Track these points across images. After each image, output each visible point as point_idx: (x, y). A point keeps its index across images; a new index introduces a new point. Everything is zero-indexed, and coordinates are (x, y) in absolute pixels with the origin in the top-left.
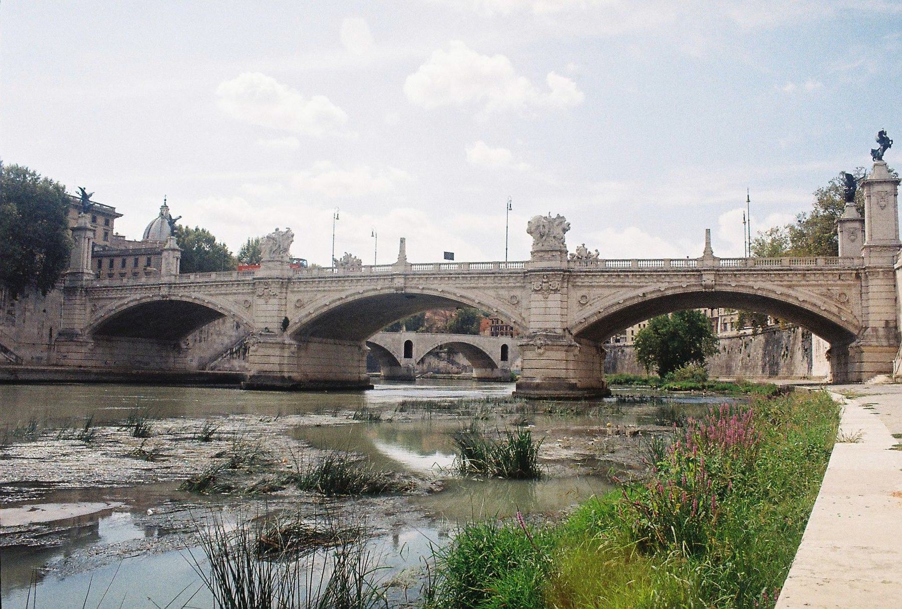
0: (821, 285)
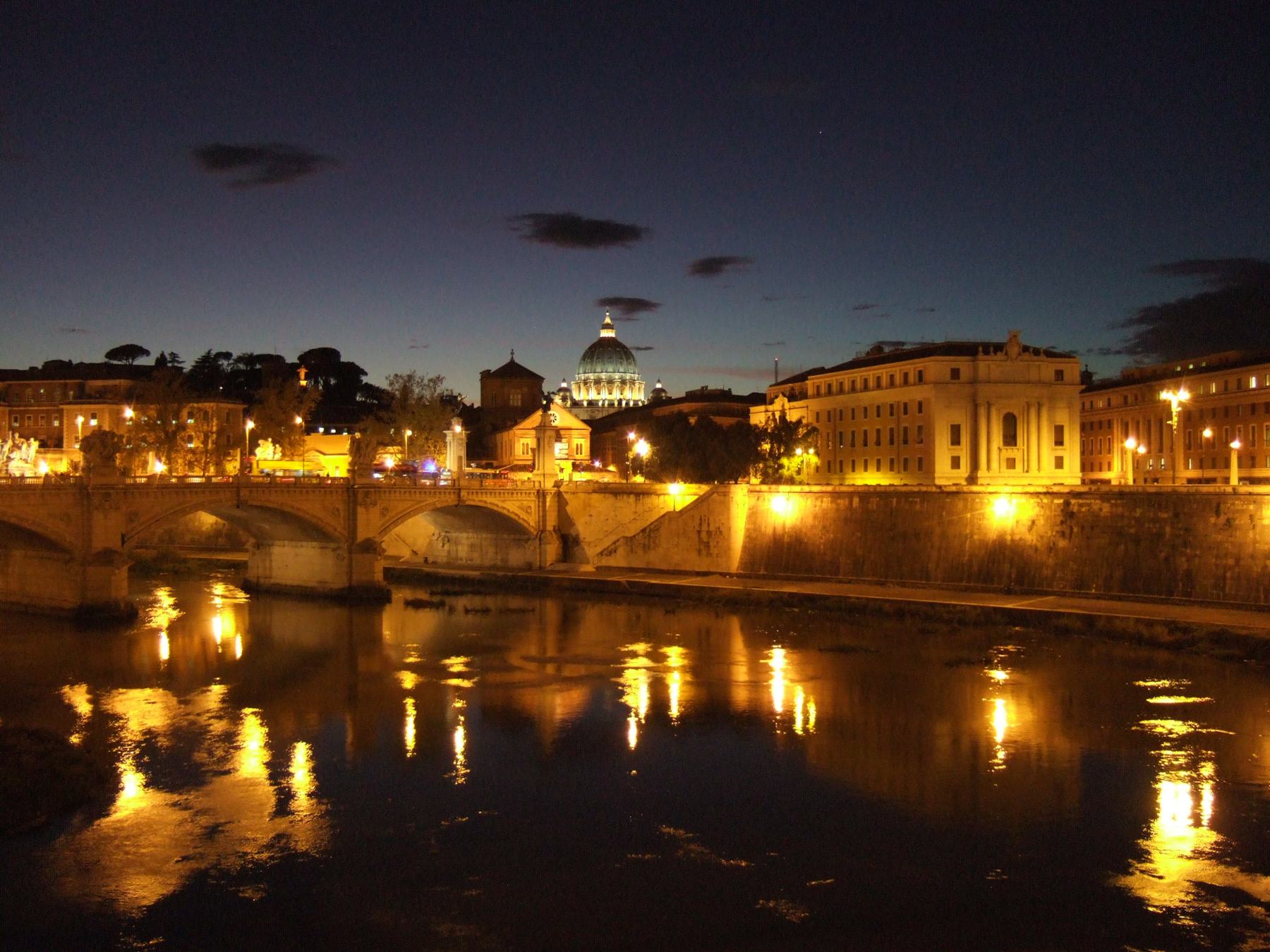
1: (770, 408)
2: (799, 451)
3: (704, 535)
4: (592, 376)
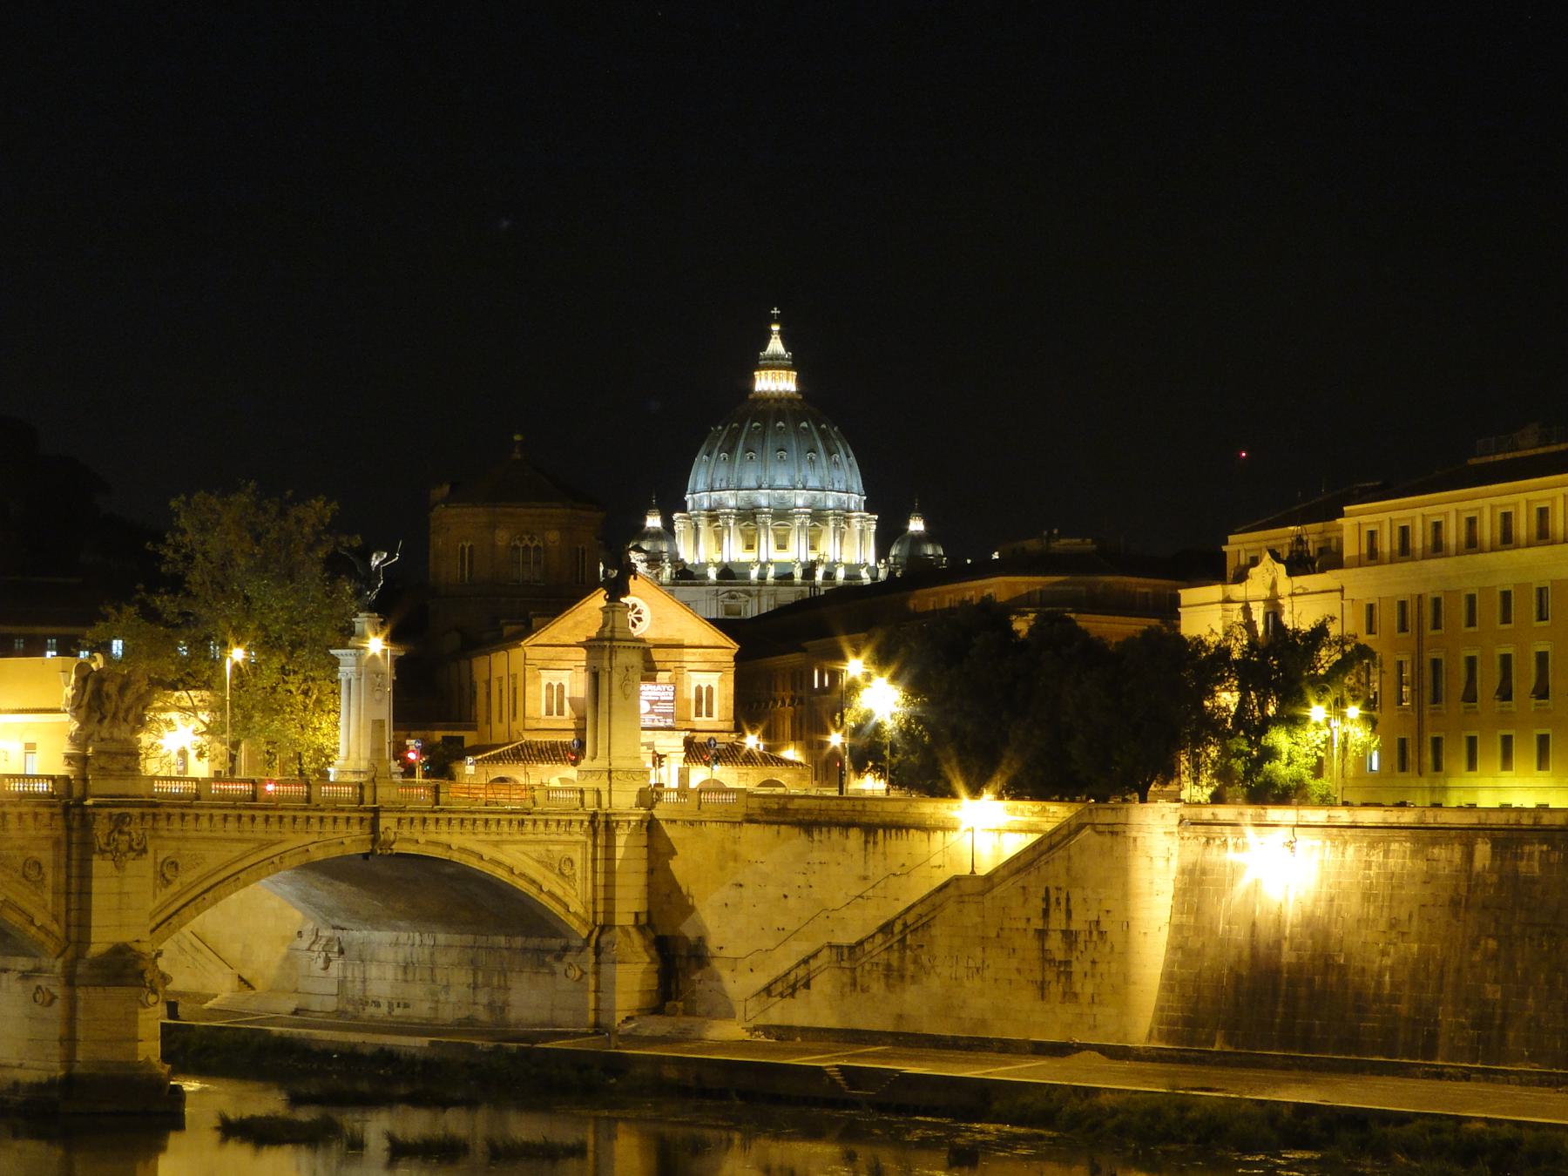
0: (539, 842)
1: (1237, 591)
2: (1317, 711)
3: (1055, 943)
4: (730, 499)
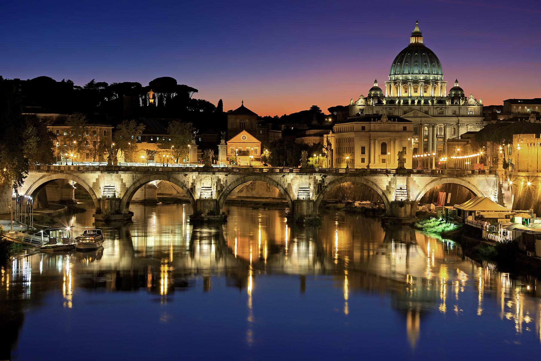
4: (400, 77)
